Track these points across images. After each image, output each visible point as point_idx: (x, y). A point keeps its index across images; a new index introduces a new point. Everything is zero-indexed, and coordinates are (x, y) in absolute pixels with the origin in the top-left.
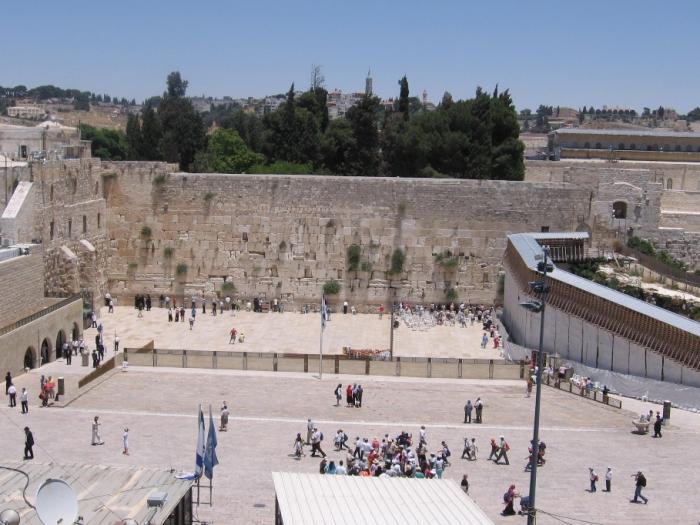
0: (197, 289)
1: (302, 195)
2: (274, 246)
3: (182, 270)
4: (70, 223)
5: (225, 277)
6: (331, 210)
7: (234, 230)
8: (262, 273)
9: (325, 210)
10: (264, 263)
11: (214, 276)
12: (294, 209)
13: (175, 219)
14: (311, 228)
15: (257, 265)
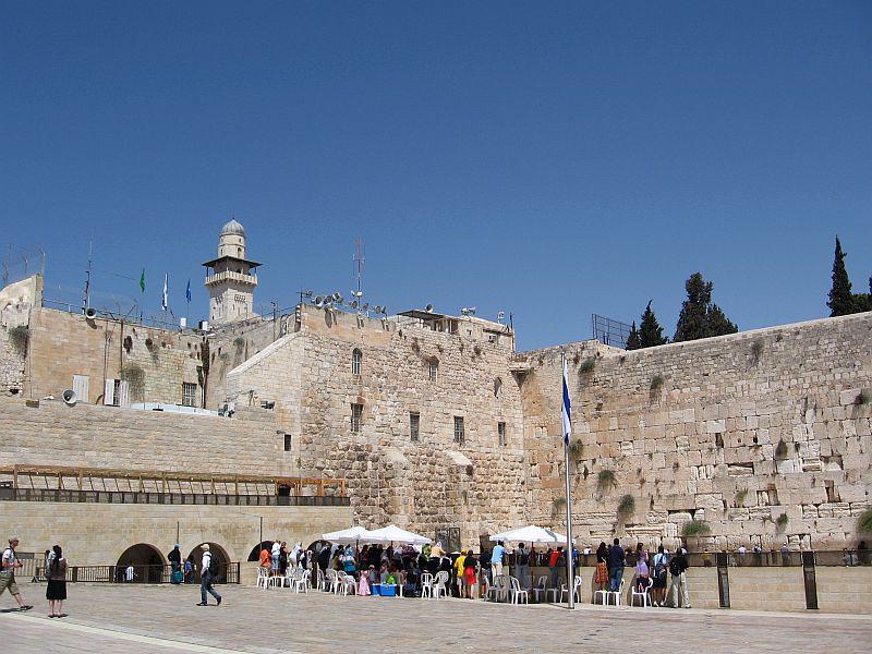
0: (652, 533)
1: (806, 355)
2: (769, 451)
3: (627, 505)
4: (415, 417)
5: (693, 512)
6: (861, 374)
7: (701, 431)
8: (750, 500)
9: (850, 375)
10: (753, 484)
11: (675, 512)
12: (794, 382)
13: (614, 424)
14: (828, 411)
15: (742, 487)
